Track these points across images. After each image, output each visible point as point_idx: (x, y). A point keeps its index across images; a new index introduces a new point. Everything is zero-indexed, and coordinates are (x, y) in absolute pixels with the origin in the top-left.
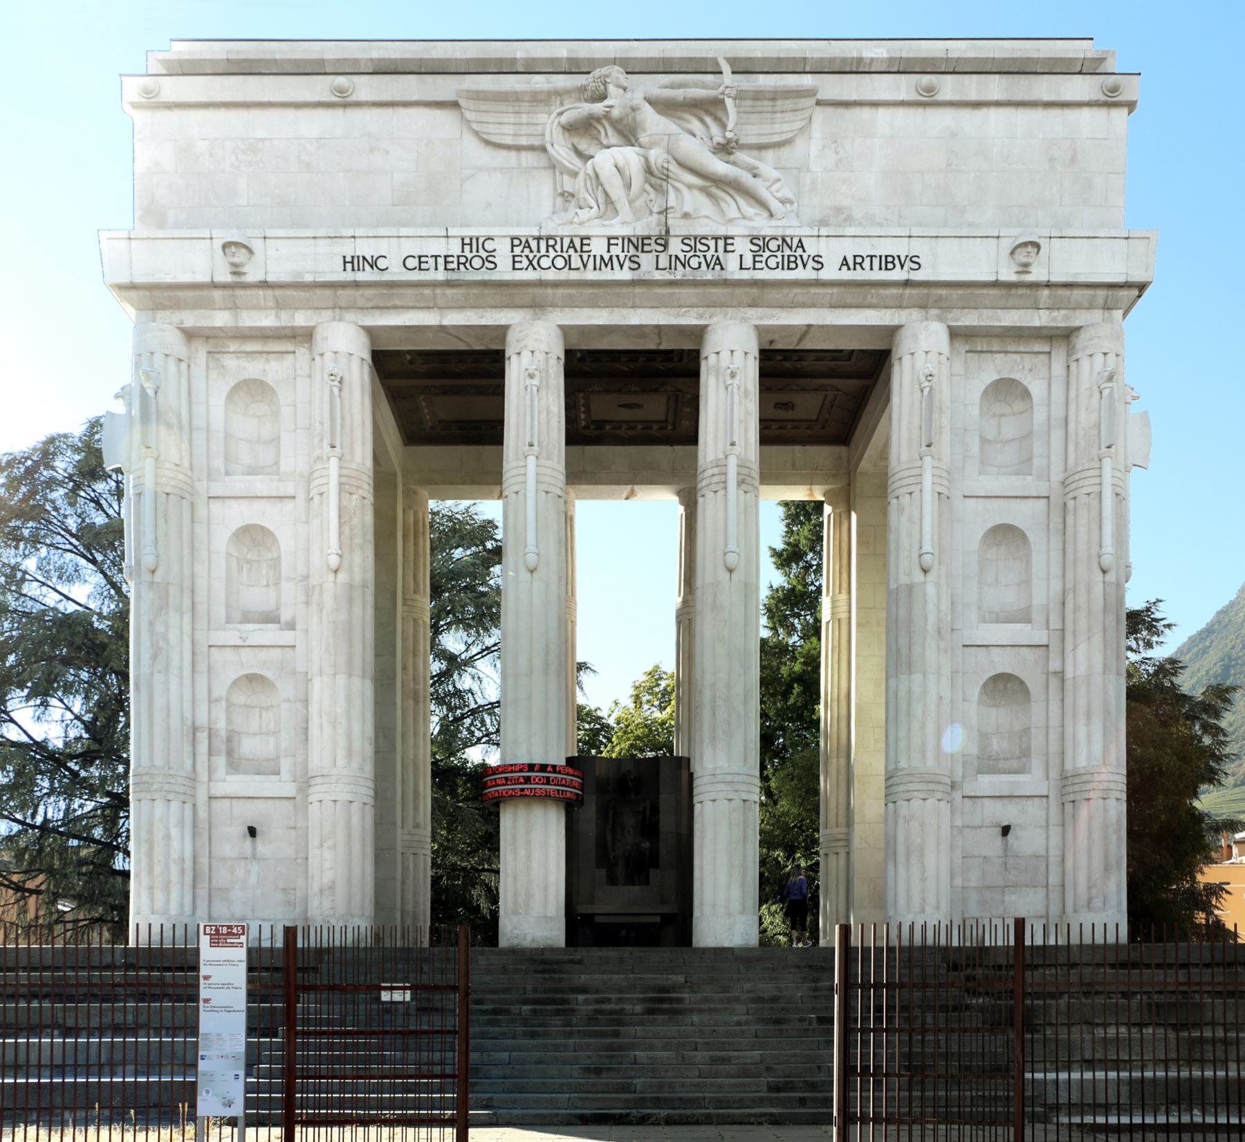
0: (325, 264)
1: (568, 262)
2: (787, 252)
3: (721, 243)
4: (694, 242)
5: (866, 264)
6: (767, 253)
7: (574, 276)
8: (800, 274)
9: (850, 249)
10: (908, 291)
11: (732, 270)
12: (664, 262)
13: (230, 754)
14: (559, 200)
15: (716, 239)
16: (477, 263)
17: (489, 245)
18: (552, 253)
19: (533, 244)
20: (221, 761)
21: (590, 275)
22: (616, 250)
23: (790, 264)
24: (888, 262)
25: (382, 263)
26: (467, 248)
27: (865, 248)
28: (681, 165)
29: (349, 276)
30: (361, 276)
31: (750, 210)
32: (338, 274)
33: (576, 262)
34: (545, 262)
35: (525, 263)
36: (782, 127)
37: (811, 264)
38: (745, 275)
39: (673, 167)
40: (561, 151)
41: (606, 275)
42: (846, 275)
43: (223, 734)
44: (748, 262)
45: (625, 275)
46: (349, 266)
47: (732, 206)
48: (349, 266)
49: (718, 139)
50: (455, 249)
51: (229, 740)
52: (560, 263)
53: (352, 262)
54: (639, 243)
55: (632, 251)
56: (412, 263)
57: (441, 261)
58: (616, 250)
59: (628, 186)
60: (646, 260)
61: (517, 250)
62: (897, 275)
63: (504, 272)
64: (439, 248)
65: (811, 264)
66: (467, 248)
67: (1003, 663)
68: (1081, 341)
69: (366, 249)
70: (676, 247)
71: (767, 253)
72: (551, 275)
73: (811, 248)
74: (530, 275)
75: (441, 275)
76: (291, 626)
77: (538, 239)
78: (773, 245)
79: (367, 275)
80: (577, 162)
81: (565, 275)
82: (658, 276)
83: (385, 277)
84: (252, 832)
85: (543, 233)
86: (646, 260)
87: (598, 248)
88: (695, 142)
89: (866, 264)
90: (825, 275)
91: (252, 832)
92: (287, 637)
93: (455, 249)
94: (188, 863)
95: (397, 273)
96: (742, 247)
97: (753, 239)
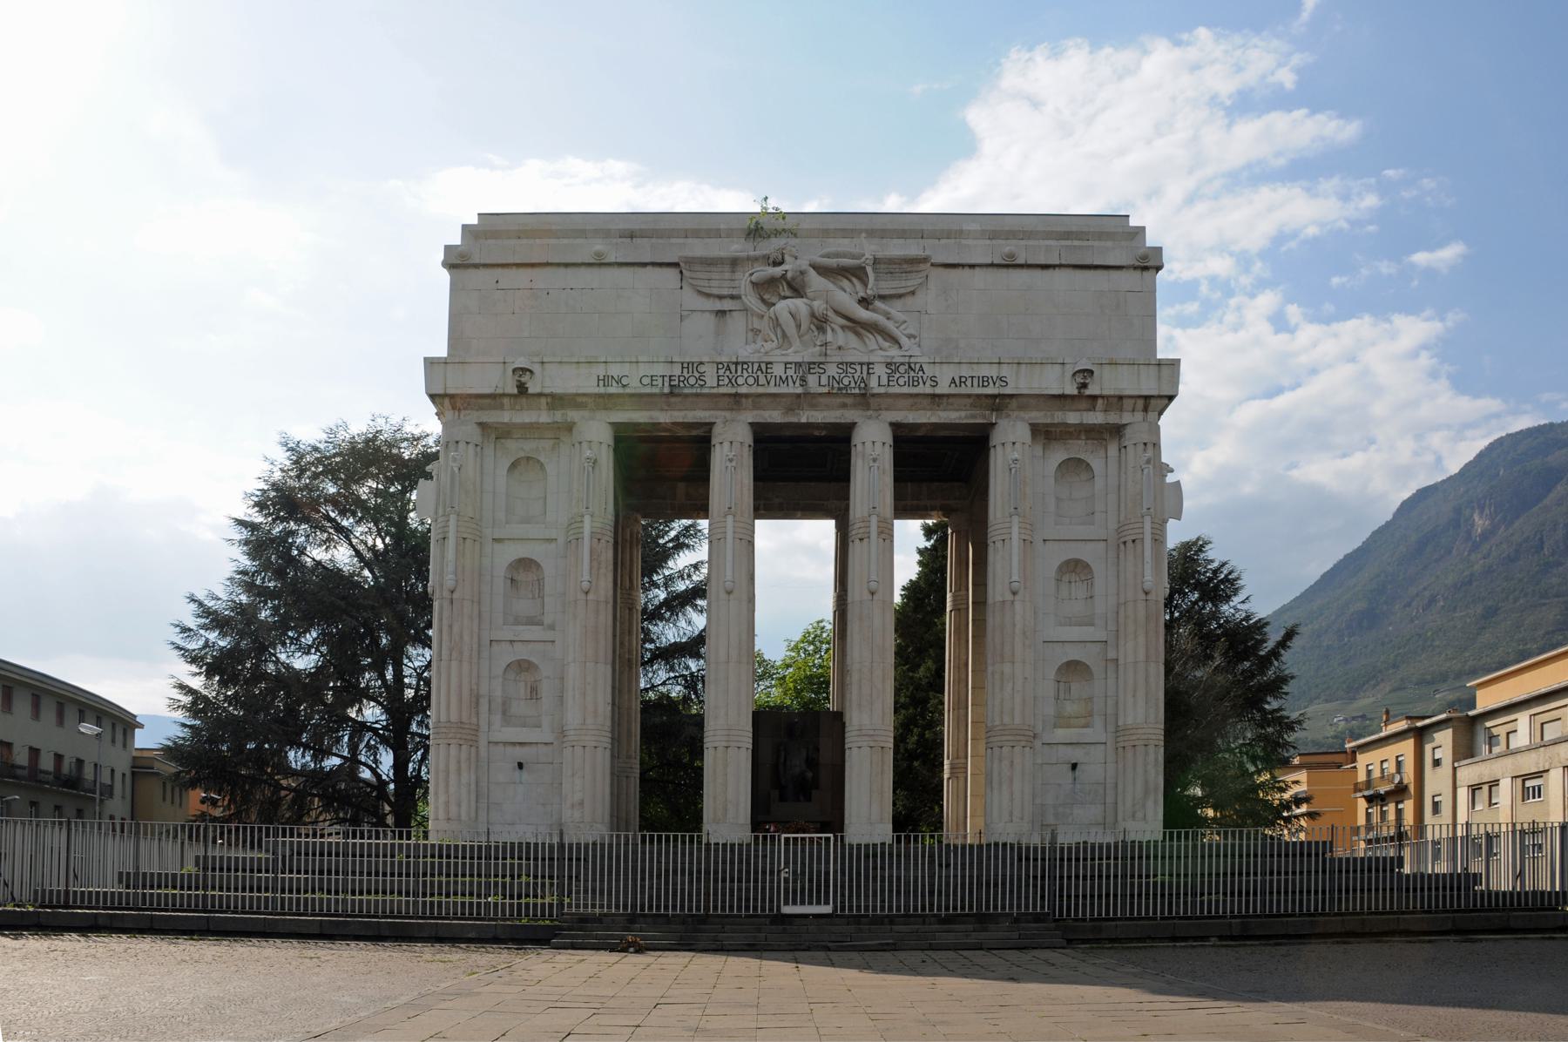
1: (757, 380)
5: (969, 383)
7: (761, 390)
8: (920, 389)
12: (824, 381)
13: (504, 713)
14: (750, 334)
15: (861, 364)
16: (692, 381)
17: (702, 369)
19: (733, 367)
20: (497, 718)
21: (772, 390)
22: (790, 372)
23: (914, 382)
27: (965, 371)
28: (837, 312)
30: (611, 390)
31: (887, 344)
33: (762, 380)
34: (740, 381)
36: (912, 283)
37: (929, 383)
39: (831, 314)
40: (752, 300)
41: (783, 389)
42: (953, 390)
43: (500, 700)
44: (884, 381)
47: (872, 341)
49: (862, 294)
51: (504, 704)
52: (751, 381)
53: (605, 380)
56: (646, 381)
59: (799, 326)
62: (990, 390)
65: (929, 383)
67: (1074, 654)
68: (1128, 431)
69: (615, 371)
76: (552, 627)
77: (737, 364)
78: (902, 369)
80: (764, 308)
83: (628, 391)
84: (520, 766)
86: (812, 380)
87: (778, 370)
88: (845, 296)
89: (969, 383)
91: (520, 766)
92: (549, 635)
93: (677, 371)
94: (473, 786)
96: (880, 370)
97: (888, 365)
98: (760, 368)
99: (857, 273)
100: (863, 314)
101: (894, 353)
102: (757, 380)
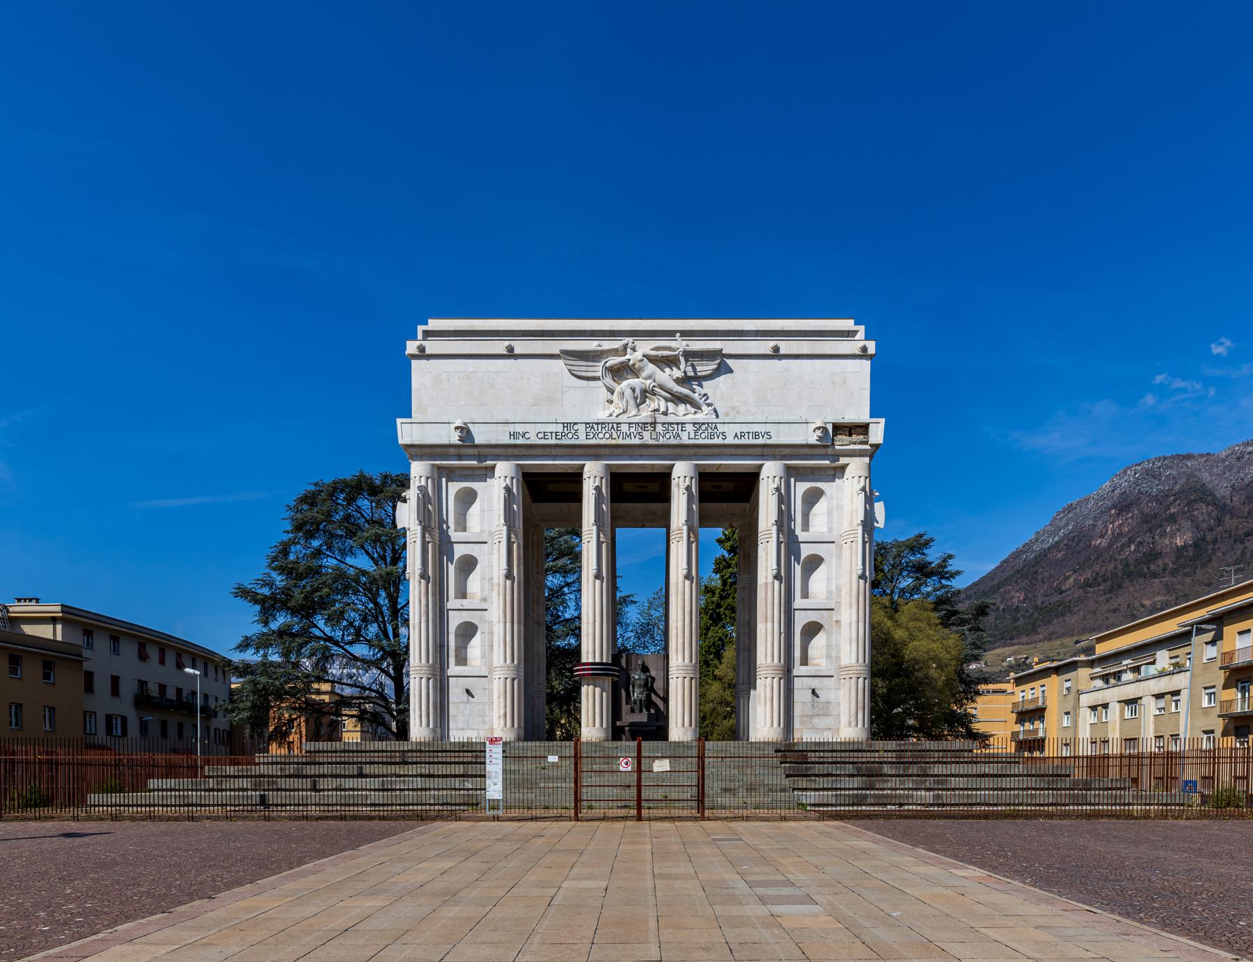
0: (501, 436)
1: (611, 436)
7: (613, 442)
9: (738, 429)
11: (685, 440)
17: (576, 427)
21: (621, 442)
22: (632, 430)
23: (711, 436)
24: (756, 435)
27: (745, 428)
29: (512, 442)
30: (517, 442)
33: (615, 435)
38: (691, 442)
41: (628, 441)
42: (737, 441)
44: (692, 436)
45: (636, 441)
50: (560, 428)
52: (607, 436)
53: (513, 435)
56: (541, 435)
60: (646, 435)
62: (761, 441)
63: (582, 440)
64: (553, 428)
69: (520, 429)
70: (659, 428)
72: (603, 442)
73: (721, 428)
74: (593, 442)
75: (554, 442)
79: (521, 441)
83: (528, 442)
86: (646, 435)
87: (624, 428)
90: (727, 442)
93: (560, 428)
95: (534, 440)
99: (670, 362)
100: (678, 389)
101: (700, 417)
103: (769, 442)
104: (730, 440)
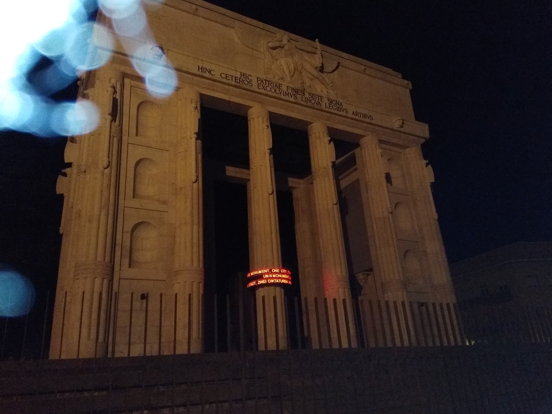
1: (275, 91)
2: (338, 106)
3: (320, 98)
4: (312, 95)
6: (332, 105)
8: (340, 113)
10: (370, 126)
12: (304, 99)
15: (318, 96)
18: (270, 87)
19: (264, 82)
23: (339, 109)
25: (213, 72)
26: (242, 76)
29: (200, 73)
32: (196, 71)
33: (278, 92)
34: (268, 89)
35: (262, 87)
41: (287, 98)
42: (353, 116)
45: (292, 99)
46: (200, 70)
48: (200, 70)
50: (238, 75)
52: (273, 90)
54: (296, 91)
55: (294, 93)
56: (223, 76)
57: (234, 78)
58: (290, 91)
61: (259, 82)
62: (367, 120)
63: (255, 87)
66: (242, 76)
70: (307, 95)
71: (332, 105)
72: (270, 93)
74: (263, 91)
75: (233, 83)
78: (334, 102)
81: (274, 94)
82: (302, 103)
85: (268, 79)
87: (284, 89)
93: (238, 75)
98: (276, 85)
102: (275, 91)
103: (372, 122)
104: (350, 115)
